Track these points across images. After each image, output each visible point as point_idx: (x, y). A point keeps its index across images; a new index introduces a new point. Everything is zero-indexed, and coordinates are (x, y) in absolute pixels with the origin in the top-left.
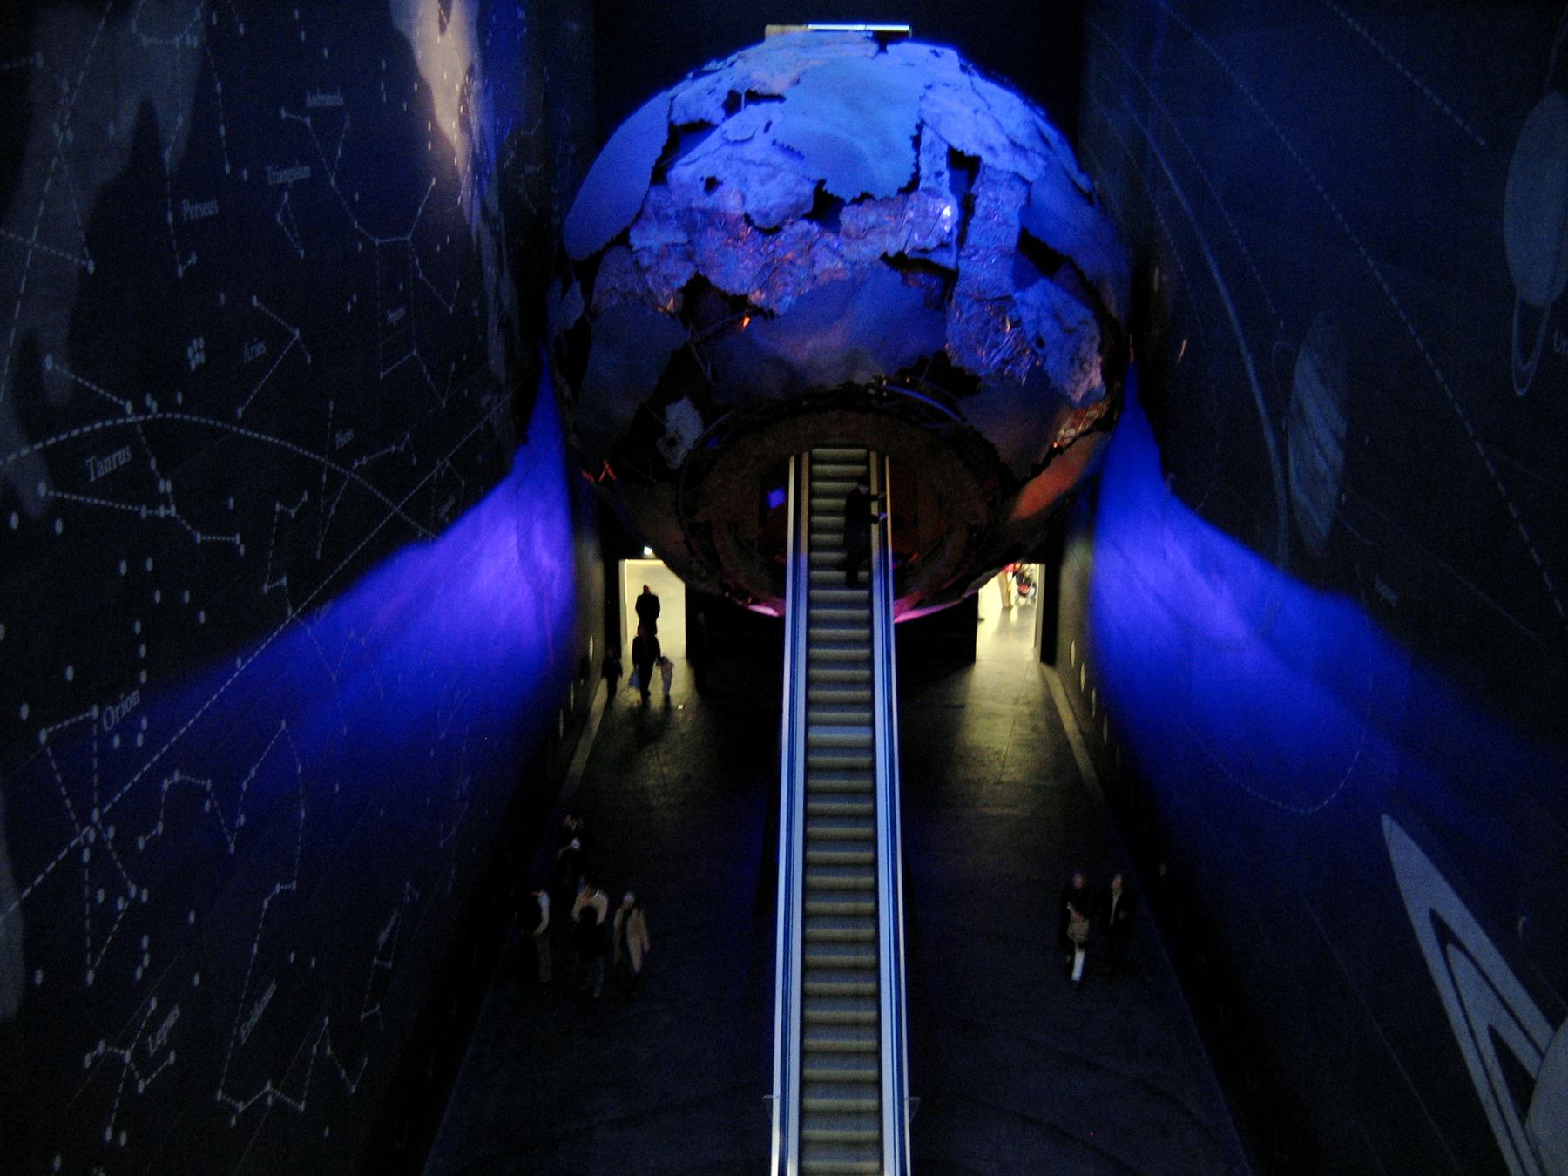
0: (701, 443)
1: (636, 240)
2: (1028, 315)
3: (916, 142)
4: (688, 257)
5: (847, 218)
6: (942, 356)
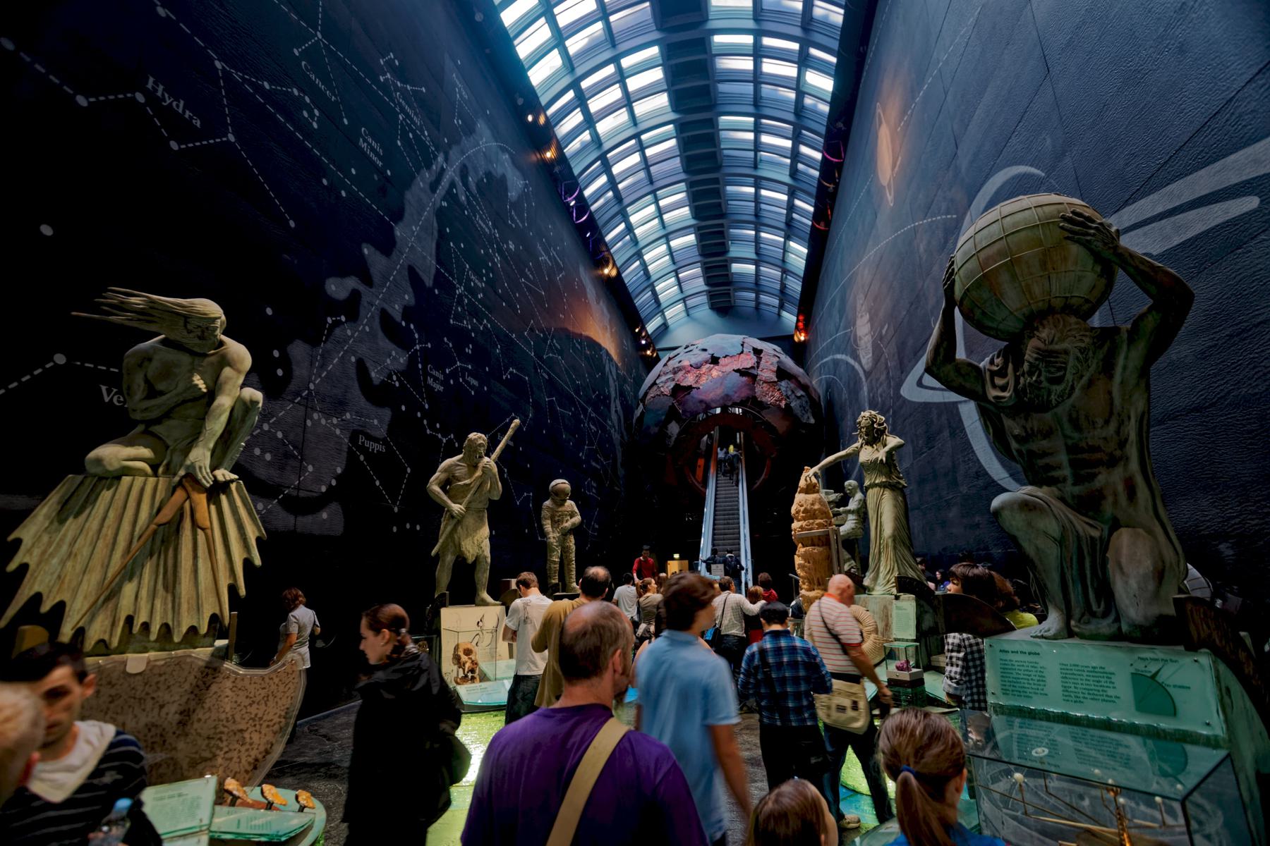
0: (679, 434)
1: (657, 382)
2: (783, 389)
3: (742, 345)
4: (674, 380)
5: (722, 361)
6: (754, 398)
